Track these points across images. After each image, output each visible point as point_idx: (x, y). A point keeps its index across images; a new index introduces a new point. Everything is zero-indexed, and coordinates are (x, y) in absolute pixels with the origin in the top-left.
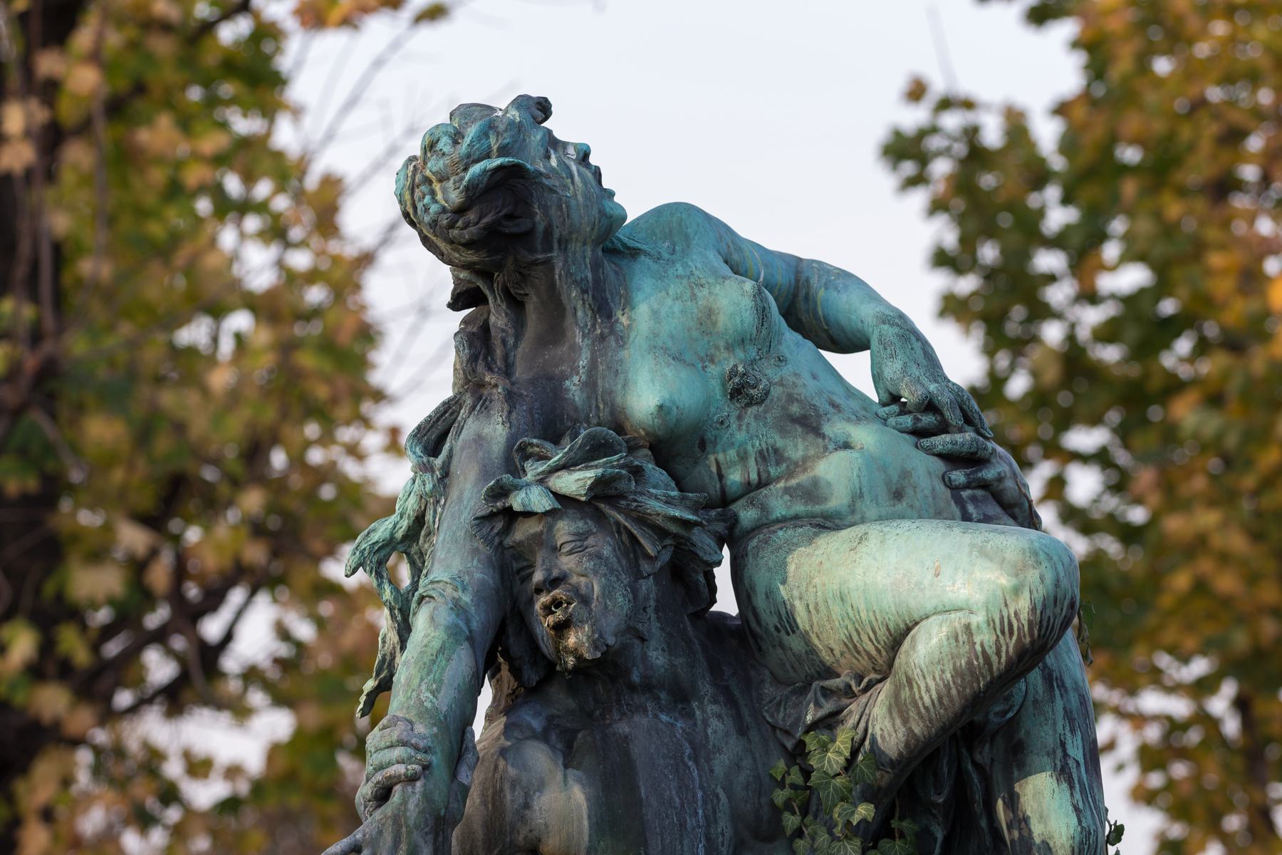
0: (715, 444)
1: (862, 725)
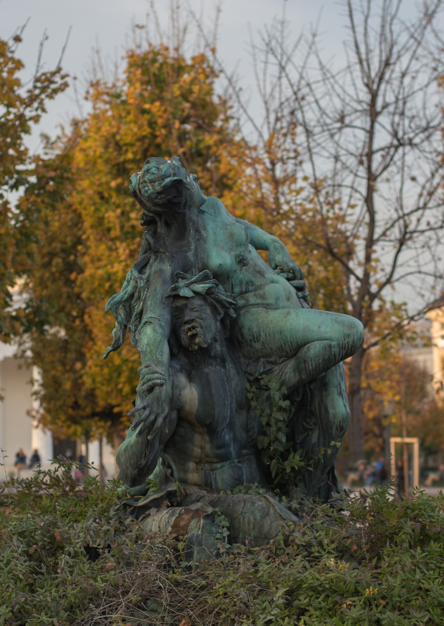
0: (232, 278)
1: (280, 374)
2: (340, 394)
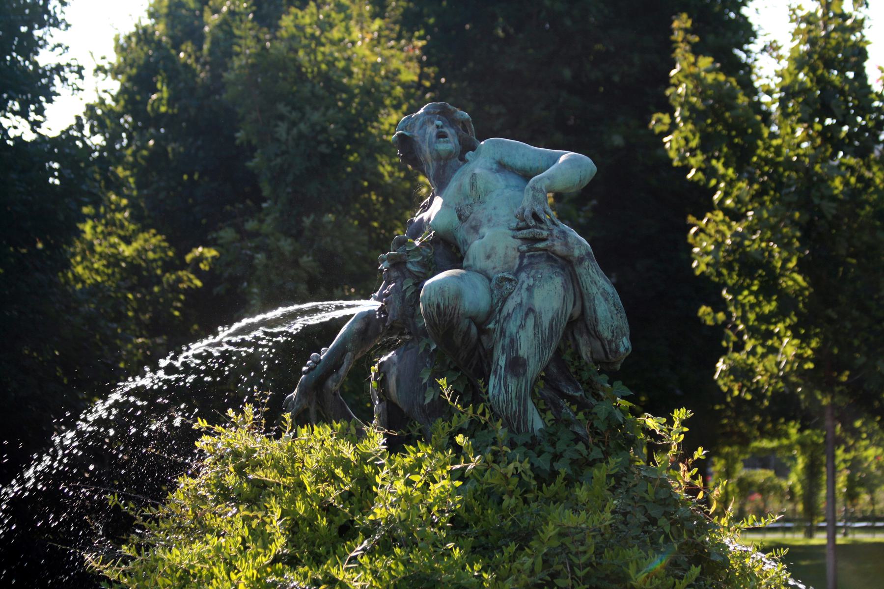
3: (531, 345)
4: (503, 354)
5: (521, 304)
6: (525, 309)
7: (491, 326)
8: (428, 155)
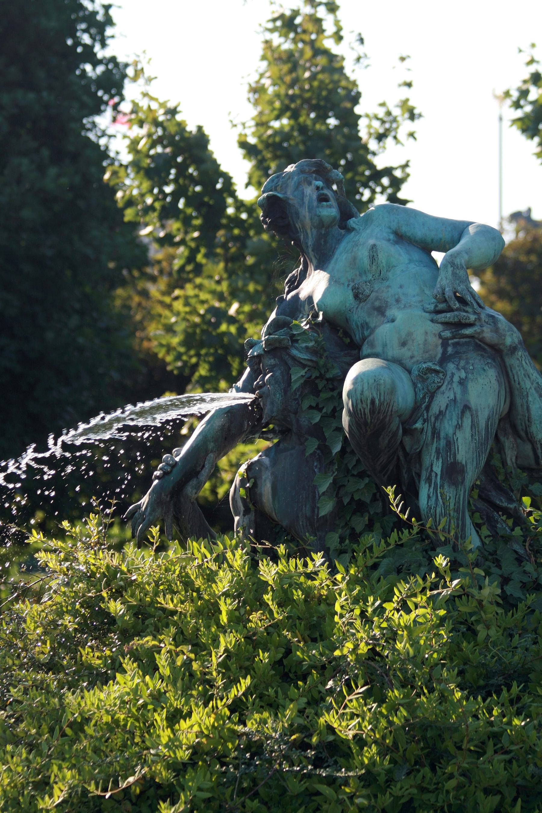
2: (429, 480)
3: (469, 449)
4: (438, 459)
5: (455, 400)
6: (460, 406)
7: (418, 425)
8: (307, 221)
